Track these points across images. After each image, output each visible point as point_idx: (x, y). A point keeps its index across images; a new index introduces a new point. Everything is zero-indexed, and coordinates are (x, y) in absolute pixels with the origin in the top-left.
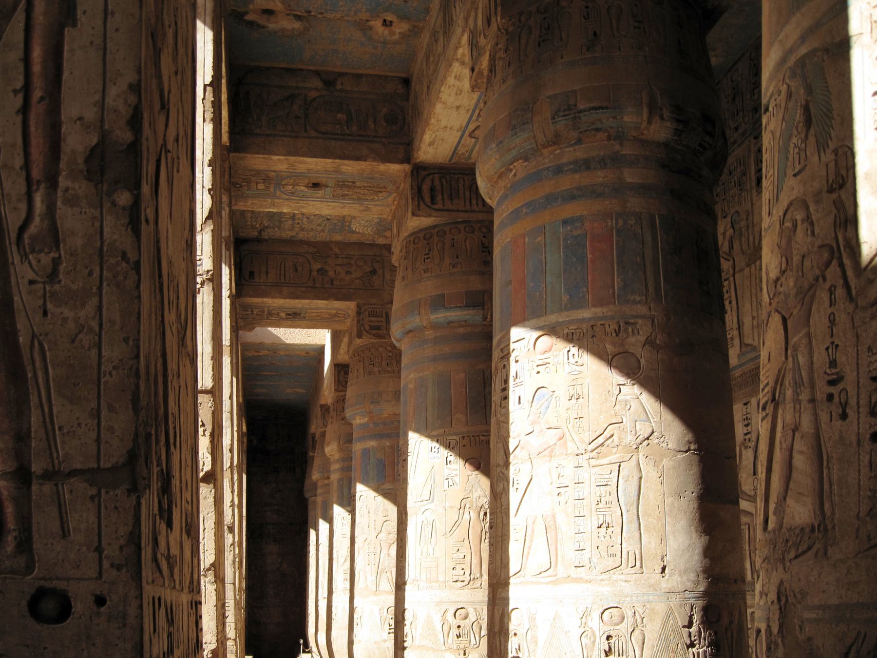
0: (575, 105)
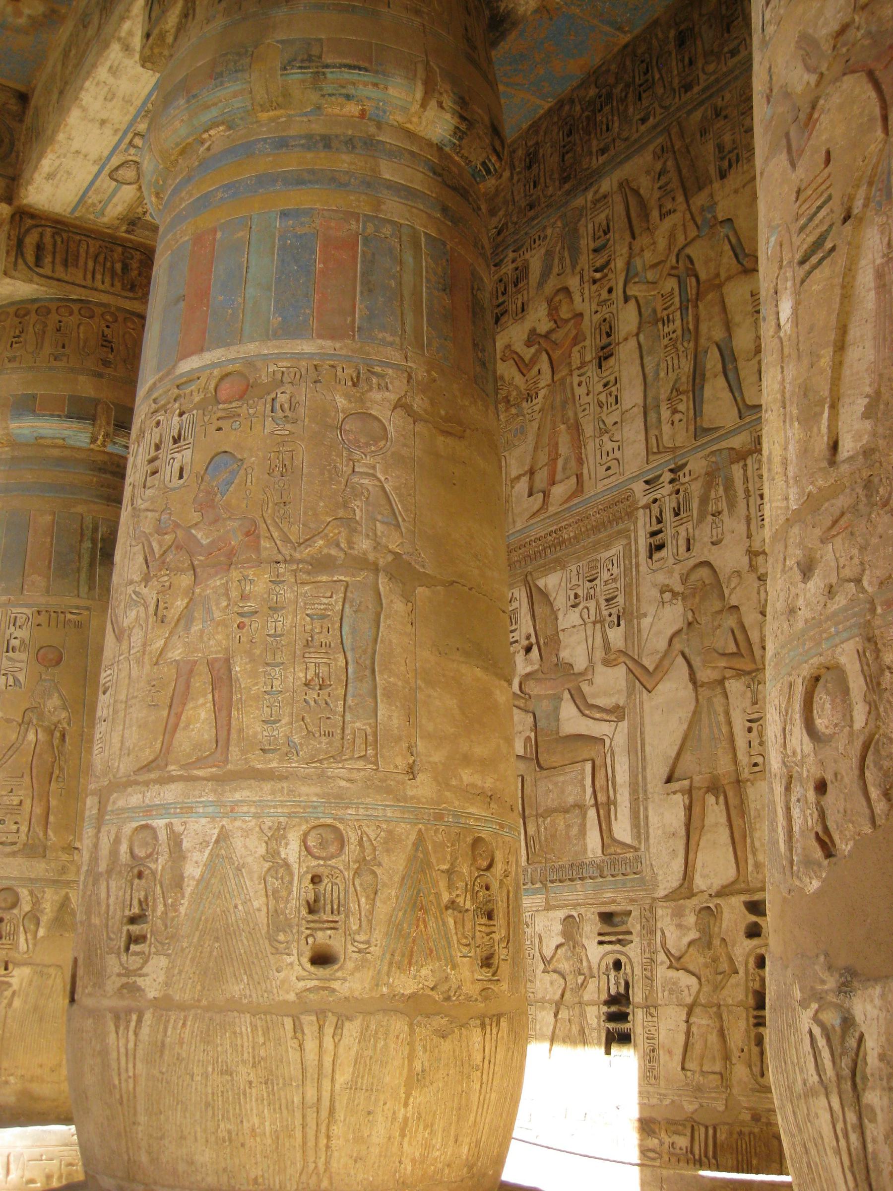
0: (320, 57)
